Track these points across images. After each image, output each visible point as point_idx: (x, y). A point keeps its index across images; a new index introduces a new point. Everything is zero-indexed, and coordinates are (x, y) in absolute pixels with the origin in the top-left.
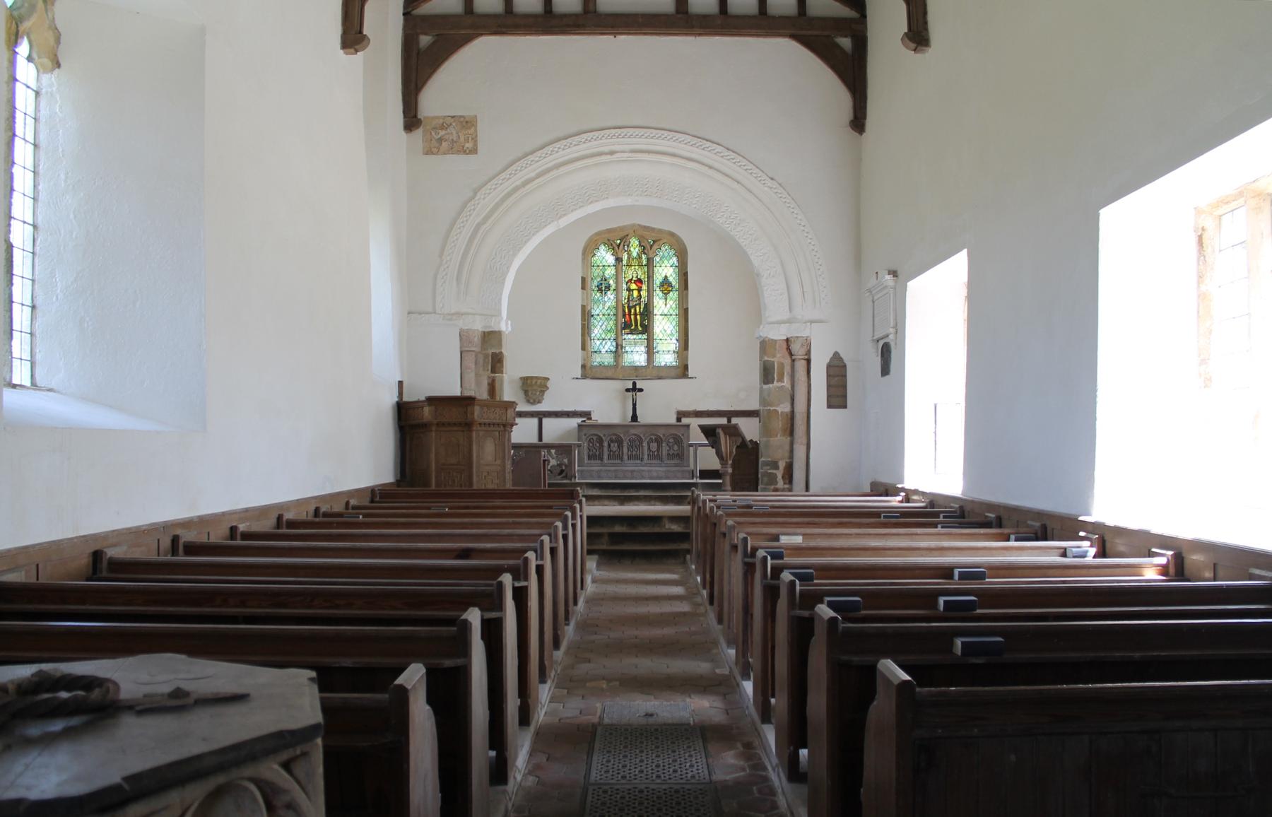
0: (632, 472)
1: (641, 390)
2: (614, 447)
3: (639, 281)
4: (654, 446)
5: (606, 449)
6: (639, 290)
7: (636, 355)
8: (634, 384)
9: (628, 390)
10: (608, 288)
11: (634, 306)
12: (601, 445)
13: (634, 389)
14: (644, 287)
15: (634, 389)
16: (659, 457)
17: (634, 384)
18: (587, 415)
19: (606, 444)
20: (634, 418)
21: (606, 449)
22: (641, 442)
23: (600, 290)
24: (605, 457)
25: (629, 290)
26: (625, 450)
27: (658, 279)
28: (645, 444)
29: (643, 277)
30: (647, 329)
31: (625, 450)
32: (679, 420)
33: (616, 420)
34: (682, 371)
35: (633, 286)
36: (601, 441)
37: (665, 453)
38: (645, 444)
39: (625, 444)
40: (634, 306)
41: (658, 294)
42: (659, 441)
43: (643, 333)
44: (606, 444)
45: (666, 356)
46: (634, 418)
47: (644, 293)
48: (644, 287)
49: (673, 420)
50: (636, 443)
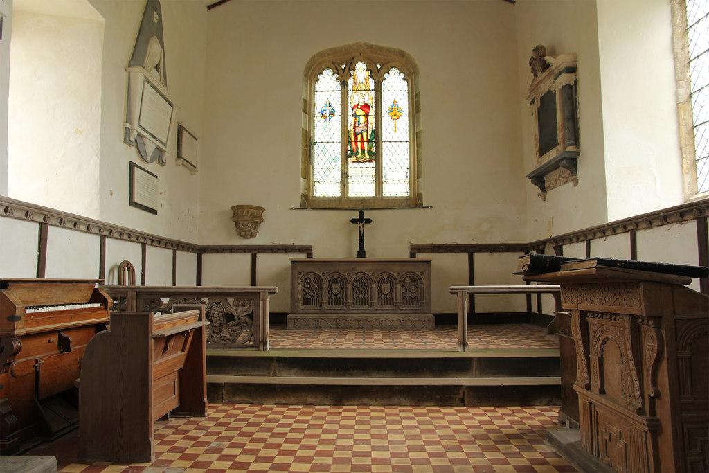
0: (359, 320)
1: (369, 221)
2: (336, 288)
3: (366, 107)
4: (386, 288)
5: (325, 291)
6: (367, 116)
7: (361, 187)
8: (361, 214)
9: (354, 221)
10: (332, 114)
11: (361, 133)
12: (320, 287)
13: (362, 220)
14: (372, 112)
15: (362, 220)
16: (392, 301)
17: (361, 214)
18: (307, 250)
19: (325, 285)
20: (362, 253)
21: (325, 291)
22: (370, 282)
23: (323, 116)
24: (325, 301)
25: (355, 116)
26: (350, 292)
27: (386, 107)
28: (374, 285)
29: (371, 102)
30: (376, 157)
31: (350, 292)
32: (413, 255)
33: (340, 255)
34: (415, 202)
35: (360, 112)
36: (319, 280)
37: (399, 296)
38: (374, 285)
39: (350, 285)
40: (361, 133)
41: (386, 121)
42: (392, 281)
43: (370, 161)
44: (325, 285)
45: (397, 186)
46: (362, 253)
47: (371, 119)
48: (372, 112)
49: (406, 255)
50: (363, 284)
